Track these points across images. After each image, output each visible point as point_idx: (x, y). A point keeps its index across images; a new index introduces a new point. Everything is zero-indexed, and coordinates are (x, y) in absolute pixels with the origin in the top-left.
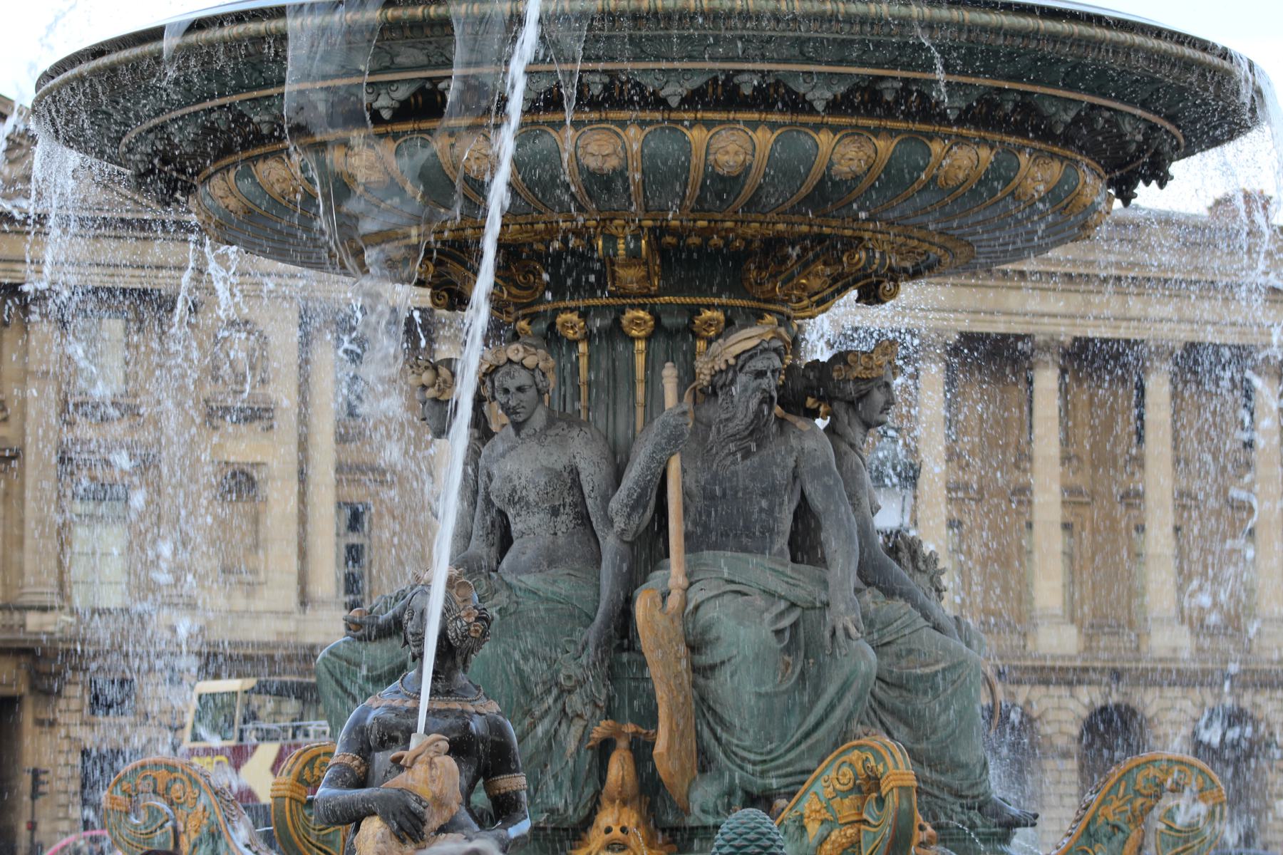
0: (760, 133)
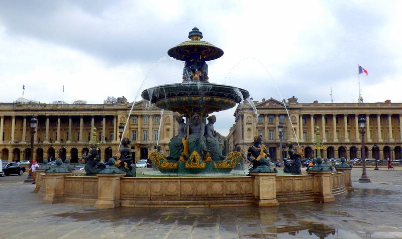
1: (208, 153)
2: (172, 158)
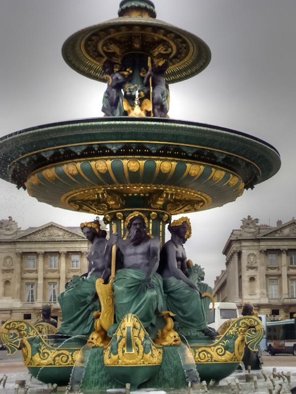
0: (108, 161)
1: (170, 323)
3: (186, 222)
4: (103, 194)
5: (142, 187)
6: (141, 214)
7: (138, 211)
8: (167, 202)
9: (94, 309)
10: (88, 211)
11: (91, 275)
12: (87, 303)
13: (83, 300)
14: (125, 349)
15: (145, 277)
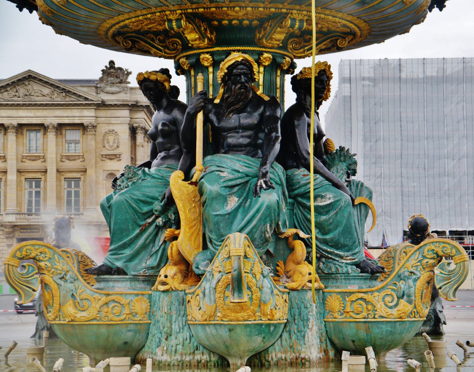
2: (120, 271)
3: (324, 70)
4: (178, 20)
5: (249, 9)
6: (247, 56)
7: (239, 51)
8: (290, 36)
9: (166, 225)
10: (146, 52)
11: (158, 165)
12: (153, 214)
13: (146, 209)
14: (228, 293)
15: (255, 169)
